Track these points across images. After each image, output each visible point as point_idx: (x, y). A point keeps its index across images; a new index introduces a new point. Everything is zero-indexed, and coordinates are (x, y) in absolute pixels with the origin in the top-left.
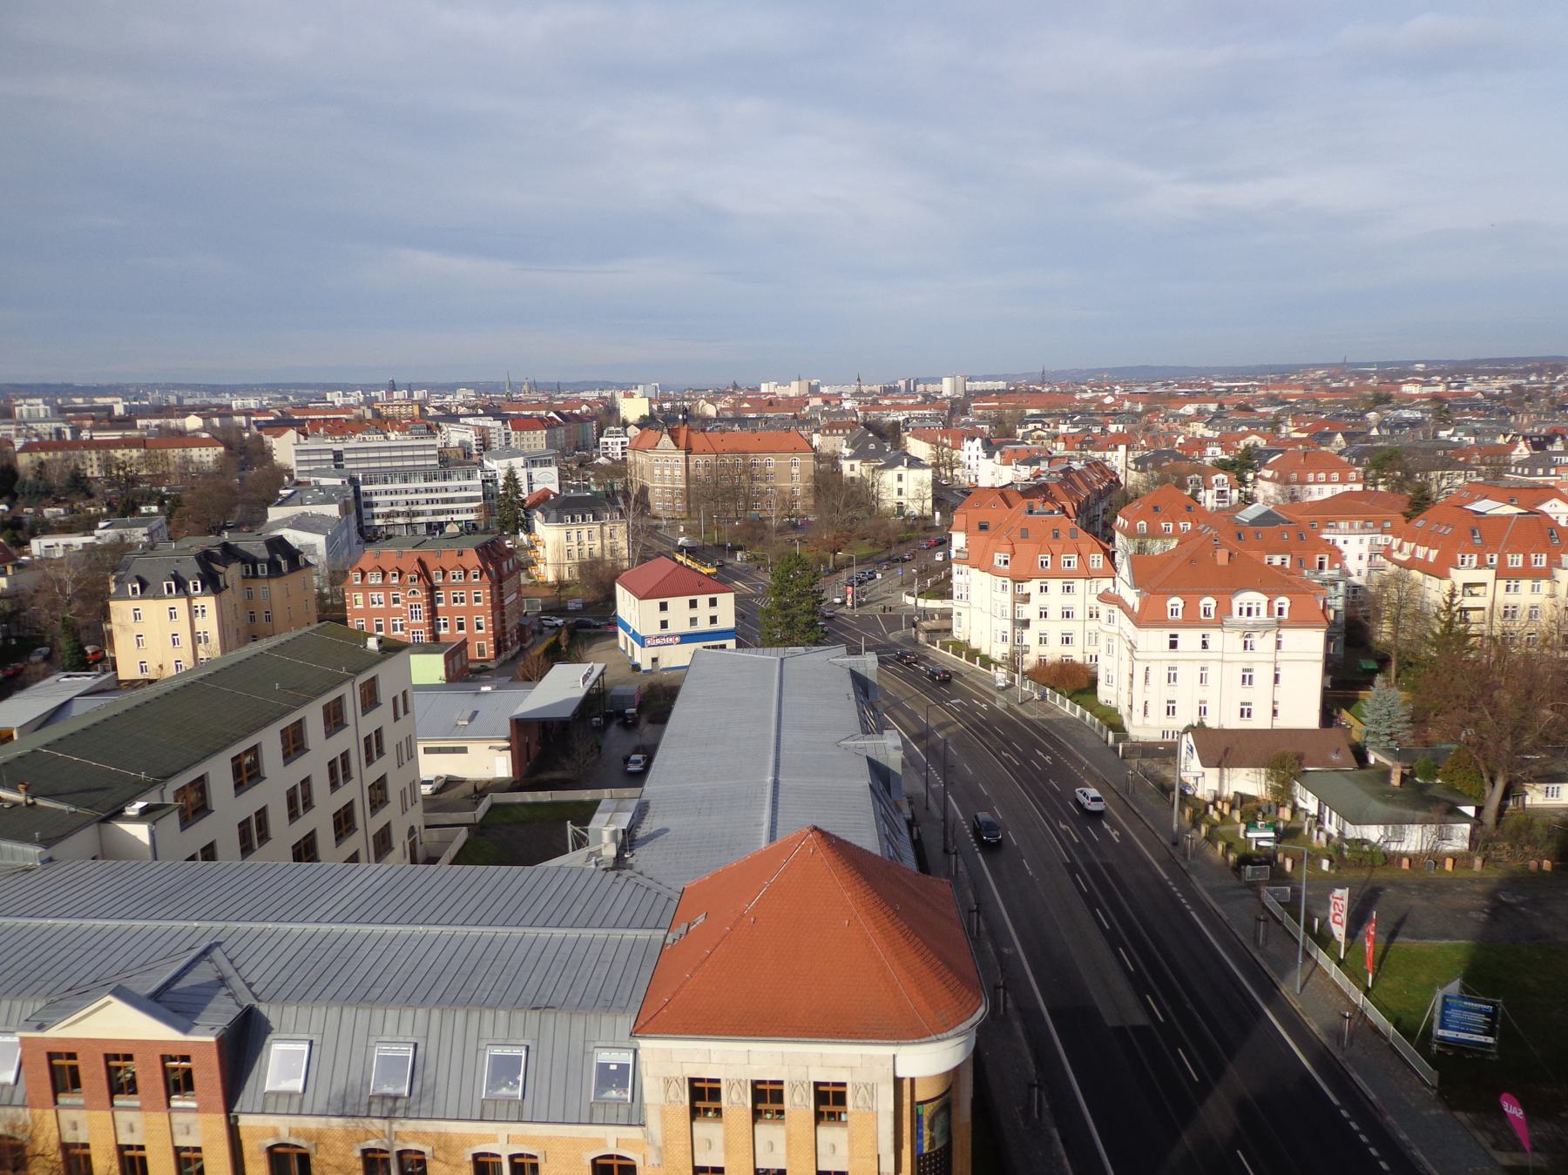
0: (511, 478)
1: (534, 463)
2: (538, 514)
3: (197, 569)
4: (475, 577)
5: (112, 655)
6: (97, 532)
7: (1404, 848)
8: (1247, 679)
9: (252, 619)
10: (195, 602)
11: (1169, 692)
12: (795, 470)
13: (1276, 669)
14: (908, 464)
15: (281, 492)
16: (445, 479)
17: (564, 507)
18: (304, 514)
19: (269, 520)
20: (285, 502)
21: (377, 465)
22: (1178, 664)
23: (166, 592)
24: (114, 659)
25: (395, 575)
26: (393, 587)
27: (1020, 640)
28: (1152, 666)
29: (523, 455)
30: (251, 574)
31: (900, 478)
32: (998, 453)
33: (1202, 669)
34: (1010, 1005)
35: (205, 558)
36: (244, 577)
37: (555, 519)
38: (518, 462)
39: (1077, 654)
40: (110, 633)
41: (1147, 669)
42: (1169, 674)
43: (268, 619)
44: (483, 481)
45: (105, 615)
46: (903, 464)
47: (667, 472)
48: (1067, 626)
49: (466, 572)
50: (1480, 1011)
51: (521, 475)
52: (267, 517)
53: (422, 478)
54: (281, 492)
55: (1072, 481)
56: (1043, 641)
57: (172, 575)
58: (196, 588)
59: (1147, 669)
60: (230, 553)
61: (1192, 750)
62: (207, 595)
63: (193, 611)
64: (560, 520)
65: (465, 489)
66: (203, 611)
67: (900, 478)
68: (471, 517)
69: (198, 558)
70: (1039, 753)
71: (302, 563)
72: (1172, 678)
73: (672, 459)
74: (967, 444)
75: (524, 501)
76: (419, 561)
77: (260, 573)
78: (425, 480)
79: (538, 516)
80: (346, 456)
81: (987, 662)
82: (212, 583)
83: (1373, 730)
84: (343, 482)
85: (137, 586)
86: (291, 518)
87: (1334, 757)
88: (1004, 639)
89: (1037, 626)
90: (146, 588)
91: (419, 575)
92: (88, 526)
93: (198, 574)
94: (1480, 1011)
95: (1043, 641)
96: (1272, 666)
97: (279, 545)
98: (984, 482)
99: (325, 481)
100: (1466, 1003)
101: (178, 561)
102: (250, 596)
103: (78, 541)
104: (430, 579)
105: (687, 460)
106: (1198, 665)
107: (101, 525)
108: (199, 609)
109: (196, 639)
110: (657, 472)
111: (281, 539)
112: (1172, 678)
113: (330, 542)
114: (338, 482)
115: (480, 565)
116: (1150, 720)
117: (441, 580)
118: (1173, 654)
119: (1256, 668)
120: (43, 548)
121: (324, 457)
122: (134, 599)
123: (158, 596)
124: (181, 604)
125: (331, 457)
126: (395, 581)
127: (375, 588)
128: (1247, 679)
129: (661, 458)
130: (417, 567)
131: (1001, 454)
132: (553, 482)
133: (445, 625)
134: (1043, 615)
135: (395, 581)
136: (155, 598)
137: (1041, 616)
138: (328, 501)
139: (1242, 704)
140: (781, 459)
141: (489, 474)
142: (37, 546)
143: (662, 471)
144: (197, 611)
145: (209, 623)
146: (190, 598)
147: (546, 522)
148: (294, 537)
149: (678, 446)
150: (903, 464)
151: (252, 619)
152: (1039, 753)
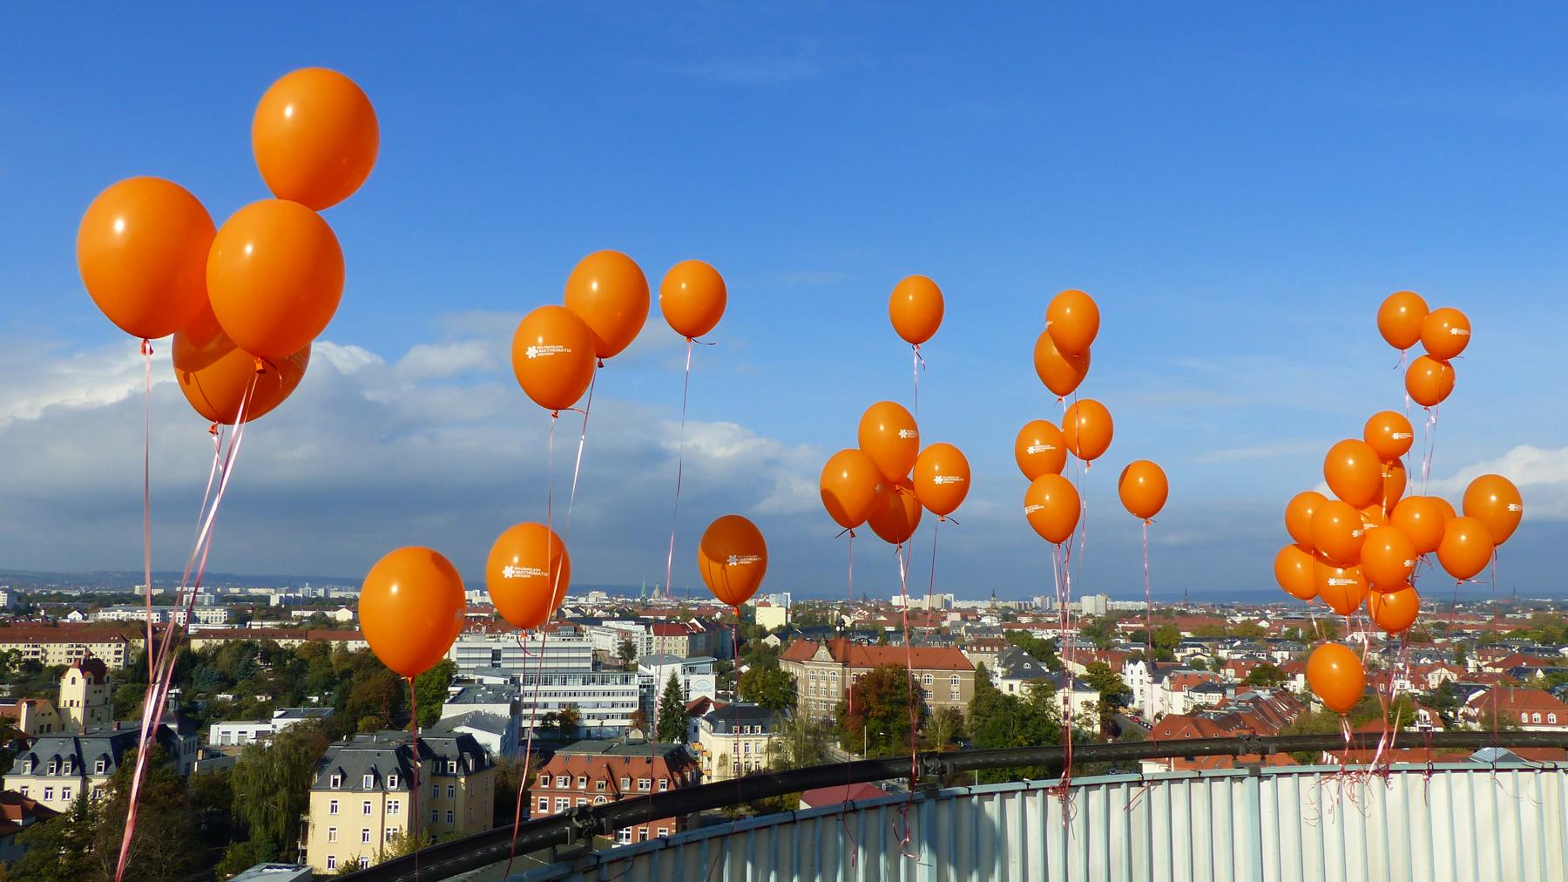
0: (673, 684)
1: (692, 670)
2: (705, 723)
3: (396, 763)
4: (663, 786)
5: (303, 848)
6: (274, 721)
9: (435, 818)
10: (388, 798)
12: (955, 688)
14: (1074, 685)
15: (450, 689)
16: (603, 683)
17: (730, 718)
18: (477, 712)
19: (442, 717)
20: (456, 700)
21: (576, 665)
23: (331, 785)
24: (304, 852)
25: (582, 780)
26: (580, 794)
29: (681, 662)
30: (440, 771)
31: (1066, 701)
32: (1166, 679)
35: (403, 753)
36: (433, 774)
37: (723, 728)
38: (678, 667)
40: (306, 825)
43: (450, 819)
44: (640, 686)
45: (305, 807)
46: (1068, 686)
47: (823, 685)
49: (653, 781)
51: (681, 681)
52: (441, 714)
53: (581, 681)
54: (450, 689)
55: (1261, 710)
57: (372, 768)
58: (392, 784)
60: (425, 751)
62: (402, 791)
63: (386, 807)
64: (728, 730)
65: (624, 695)
66: (396, 807)
67: (1066, 701)
68: (627, 722)
69: (398, 752)
71: (487, 763)
73: (828, 671)
74: (1130, 667)
75: (684, 708)
76: (608, 767)
77: (449, 771)
78: (584, 683)
79: (703, 723)
80: (504, 655)
82: (408, 780)
84: (505, 682)
85: (339, 777)
86: (466, 715)
90: (349, 783)
91: (607, 782)
92: (263, 714)
93: (396, 769)
97: (467, 742)
98: (1178, 711)
99: (488, 680)
101: (378, 755)
102: (436, 794)
103: (252, 729)
104: (616, 786)
105: (844, 673)
107: (277, 713)
108: (392, 804)
109: (386, 836)
110: (812, 684)
111: (470, 736)
113: (503, 740)
114: (500, 681)
115: (668, 774)
117: (627, 788)
120: (220, 733)
121: (483, 655)
122: (368, 792)
123: (357, 788)
124: (376, 798)
125: (490, 655)
126: (583, 786)
127: (562, 793)
129: (818, 670)
130: (605, 773)
131: (1171, 679)
132: (710, 690)
133: (628, 836)
135: (583, 786)
136: (353, 790)
138: (497, 700)
140: (941, 675)
141: (646, 679)
142: (217, 733)
143: (818, 683)
144: (390, 807)
145: (400, 820)
146: (385, 793)
147: (714, 731)
148: (481, 737)
149: (834, 657)
150: (1068, 686)
151: (435, 818)
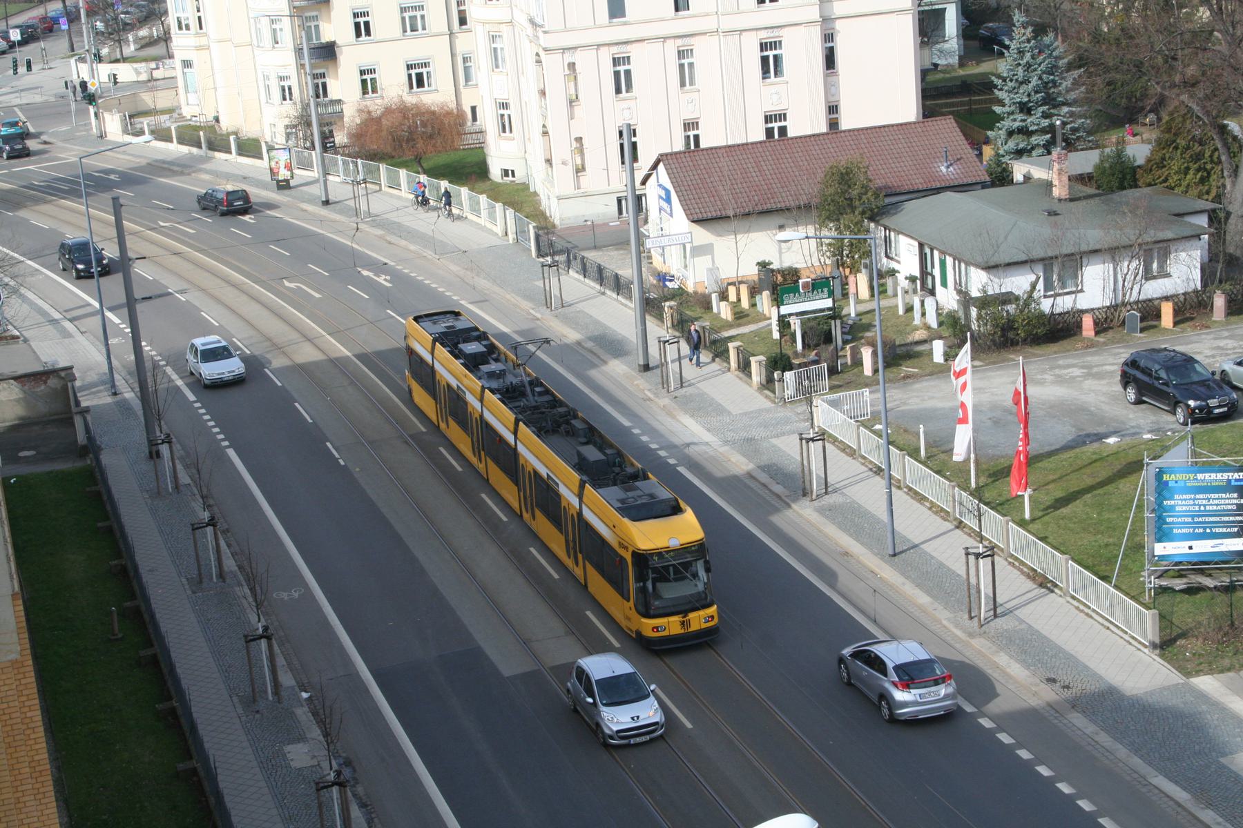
7: (1084, 302)
8: (770, 65)
11: (620, 112)
13: (829, 37)
22: (634, 51)
27: (321, 90)
28: (578, 58)
33: (681, 54)
34: (230, 564)
39: (438, 95)
41: (609, 185)
42: (617, 74)
48: (416, 49)
50: (1228, 487)
56: (368, 85)
59: (572, 66)
61: (668, 199)
70: (365, 273)
72: (623, 83)
81: (250, 148)
83: (1017, 124)
87: (943, 169)
88: (286, 93)
89: (352, 57)
94: (1228, 487)
95: (368, 85)
96: (816, 33)
100: (1200, 476)
106: (672, 47)
112: (623, 83)
116: (592, 180)
118: (619, 32)
119: (786, 36)
128: (770, 65)
134: (362, 29)
137: (358, 34)
139: (768, 119)
152: (365, 273)
